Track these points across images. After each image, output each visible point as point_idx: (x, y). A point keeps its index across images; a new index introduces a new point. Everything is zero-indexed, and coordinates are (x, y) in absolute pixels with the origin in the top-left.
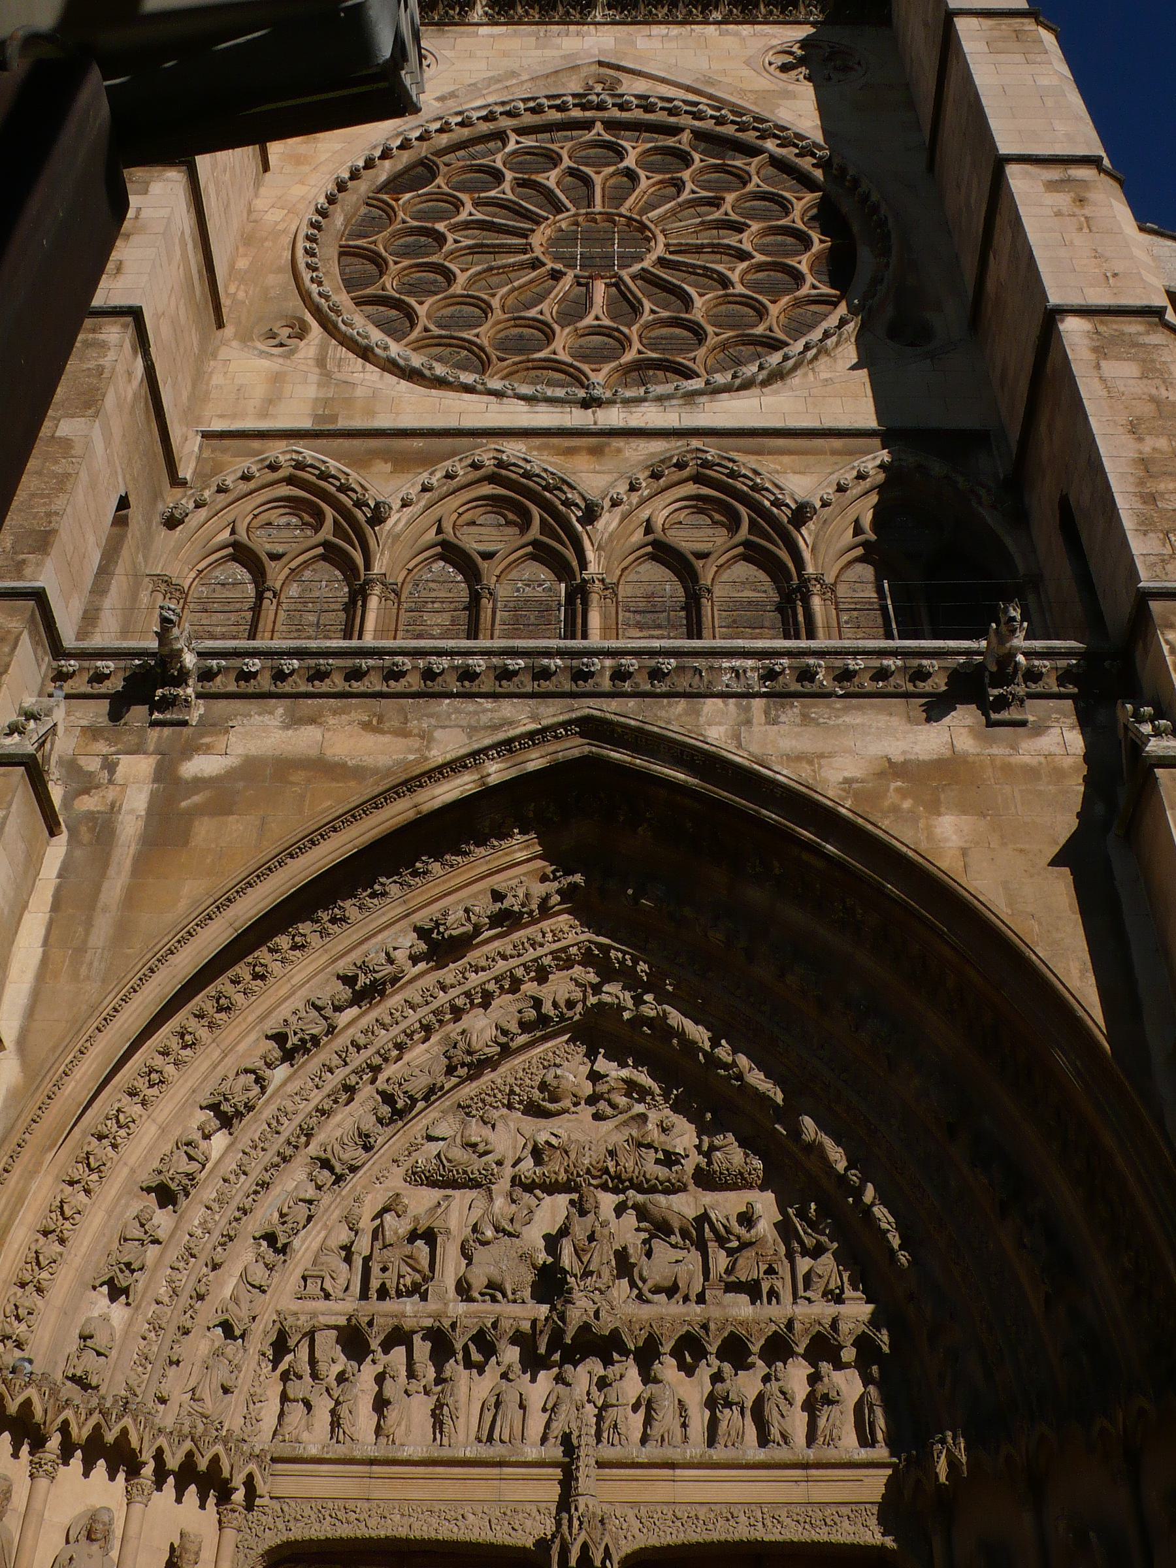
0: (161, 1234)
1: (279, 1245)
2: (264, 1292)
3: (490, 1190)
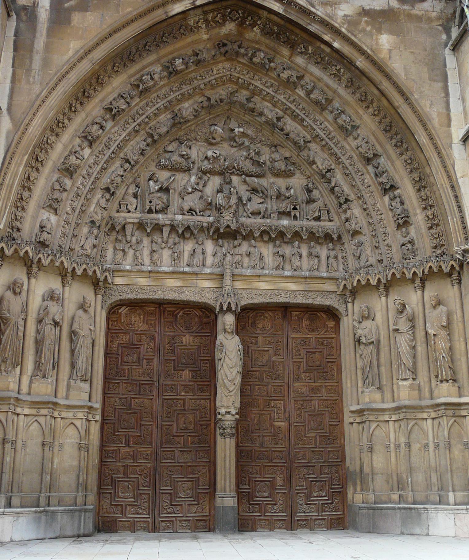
0: (68, 188)
1: (111, 192)
2: (106, 210)
3: (190, 173)
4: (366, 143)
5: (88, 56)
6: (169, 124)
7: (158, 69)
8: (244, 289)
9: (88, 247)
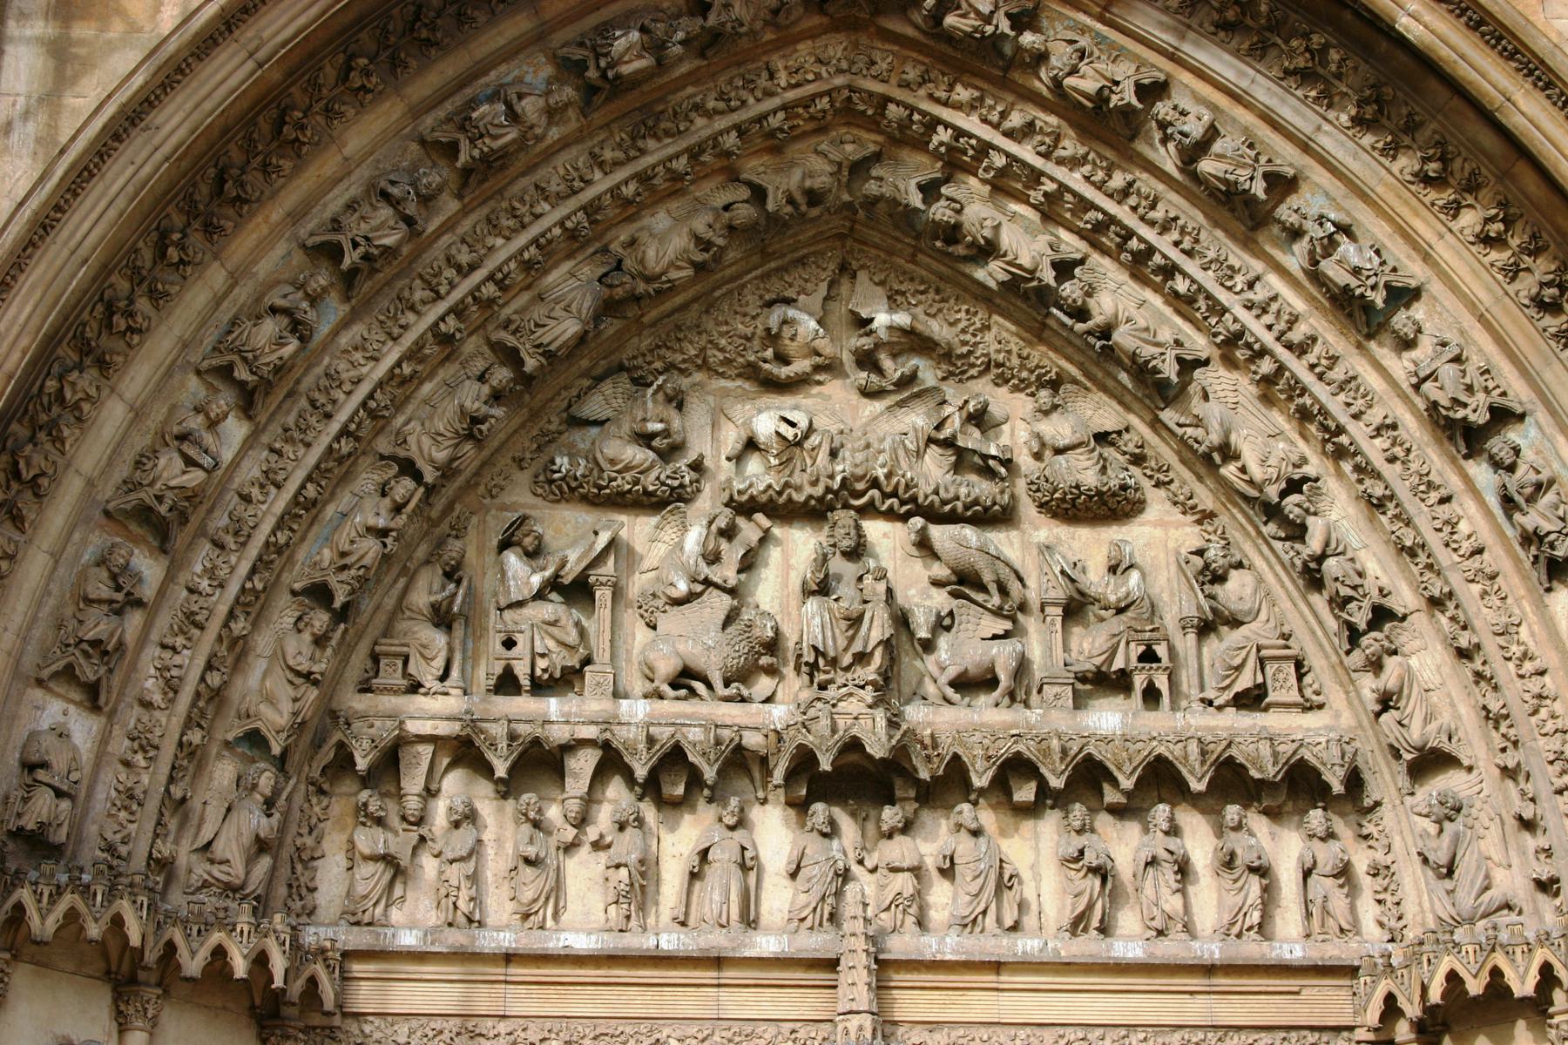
0: (148, 592)
1: (337, 604)
2: (316, 683)
4: (1457, 359)
5: (237, 33)
6: (586, 303)
7: (536, 72)
8: (933, 1025)
9: (231, 847)
